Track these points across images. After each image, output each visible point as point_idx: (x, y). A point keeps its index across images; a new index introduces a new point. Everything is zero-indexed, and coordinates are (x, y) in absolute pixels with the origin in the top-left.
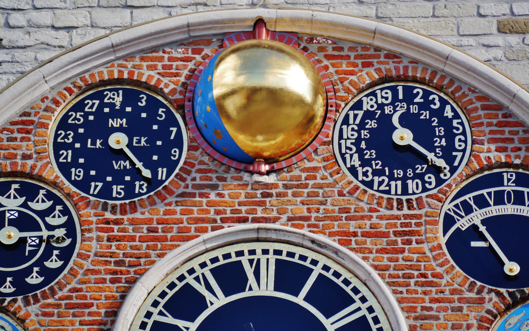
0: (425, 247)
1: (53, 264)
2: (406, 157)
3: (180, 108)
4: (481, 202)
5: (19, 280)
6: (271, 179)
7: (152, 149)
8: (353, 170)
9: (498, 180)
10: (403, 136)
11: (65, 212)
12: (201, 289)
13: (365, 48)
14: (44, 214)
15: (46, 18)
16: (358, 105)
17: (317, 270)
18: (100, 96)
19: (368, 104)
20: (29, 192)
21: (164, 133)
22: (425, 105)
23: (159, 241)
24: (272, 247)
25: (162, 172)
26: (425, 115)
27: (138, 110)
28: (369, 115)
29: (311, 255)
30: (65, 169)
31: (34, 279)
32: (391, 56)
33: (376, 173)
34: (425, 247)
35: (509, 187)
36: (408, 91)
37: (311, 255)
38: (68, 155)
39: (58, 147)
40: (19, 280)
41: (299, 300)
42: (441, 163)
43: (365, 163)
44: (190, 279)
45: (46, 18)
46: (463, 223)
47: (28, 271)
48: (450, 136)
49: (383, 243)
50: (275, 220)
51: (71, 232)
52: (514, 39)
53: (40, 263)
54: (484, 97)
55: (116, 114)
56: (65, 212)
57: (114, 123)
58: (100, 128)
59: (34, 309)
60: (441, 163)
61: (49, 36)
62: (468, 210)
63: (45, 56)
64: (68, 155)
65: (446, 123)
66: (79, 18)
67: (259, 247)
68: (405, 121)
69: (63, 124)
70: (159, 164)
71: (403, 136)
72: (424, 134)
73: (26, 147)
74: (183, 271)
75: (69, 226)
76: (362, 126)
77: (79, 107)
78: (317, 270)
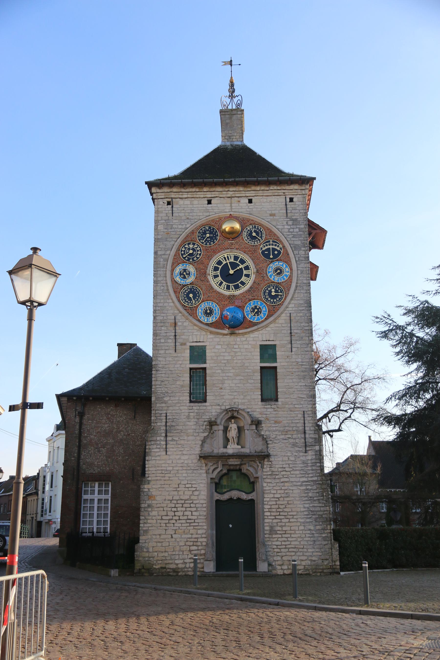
0: (258, 253)
1: (198, 256)
2: (255, 238)
3: (218, 229)
4: (267, 245)
5: (193, 259)
6: (233, 242)
7: (214, 237)
8: (246, 240)
9: (269, 241)
10: (254, 234)
11: (200, 247)
12: (222, 260)
13: (248, 219)
14: (196, 248)
15: (195, 214)
16: (247, 229)
17: (240, 257)
18: (205, 227)
19: (248, 229)
20: (194, 244)
21: (215, 234)
22: (258, 229)
23: (215, 252)
24: (233, 253)
25: (215, 241)
26: (258, 230)
27: (211, 230)
28: (248, 230)
29: (239, 255)
30: (200, 240)
31: (195, 259)
32: (252, 220)
33: (250, 240)
34: (258, 253)
35: (271, 243)
36: (255, 226)
37: (239, 255)
38: (200, 238)
39: (198, 236)
40: (193, 259)
41: (238, 262)
42: (260, 239)
43: (248, 239)
44: (220, 259)
45: (195, 214)
46: (264, 249)
47: (194, 258)
48: (262, 234)
49: (251, 252)
50: (233, 249)
51: (201, 251)
52: (272, 217)
53: (196, 256)
54: (267, 227)
55: (207, 231)
56: (200, 247)
57: (207, 232)
58: (205, 233)
59: (195, 264)
60: (260, 239)
61: (195, 217)
62: (265, 247)
63: (196, 221)
64: (200, 238)
65: (261, 232)
66: (201, 214)
67: (231, 253)
68: (255, 231)
69: (199, 233)
70: (215, 239)
71: (254, 234)
72: (257, 233)
73: (193, 237)
74: (219, 257)
75: (200, 250)
76: (247, 232)
77: (201, 229)
78: (240, 257)
